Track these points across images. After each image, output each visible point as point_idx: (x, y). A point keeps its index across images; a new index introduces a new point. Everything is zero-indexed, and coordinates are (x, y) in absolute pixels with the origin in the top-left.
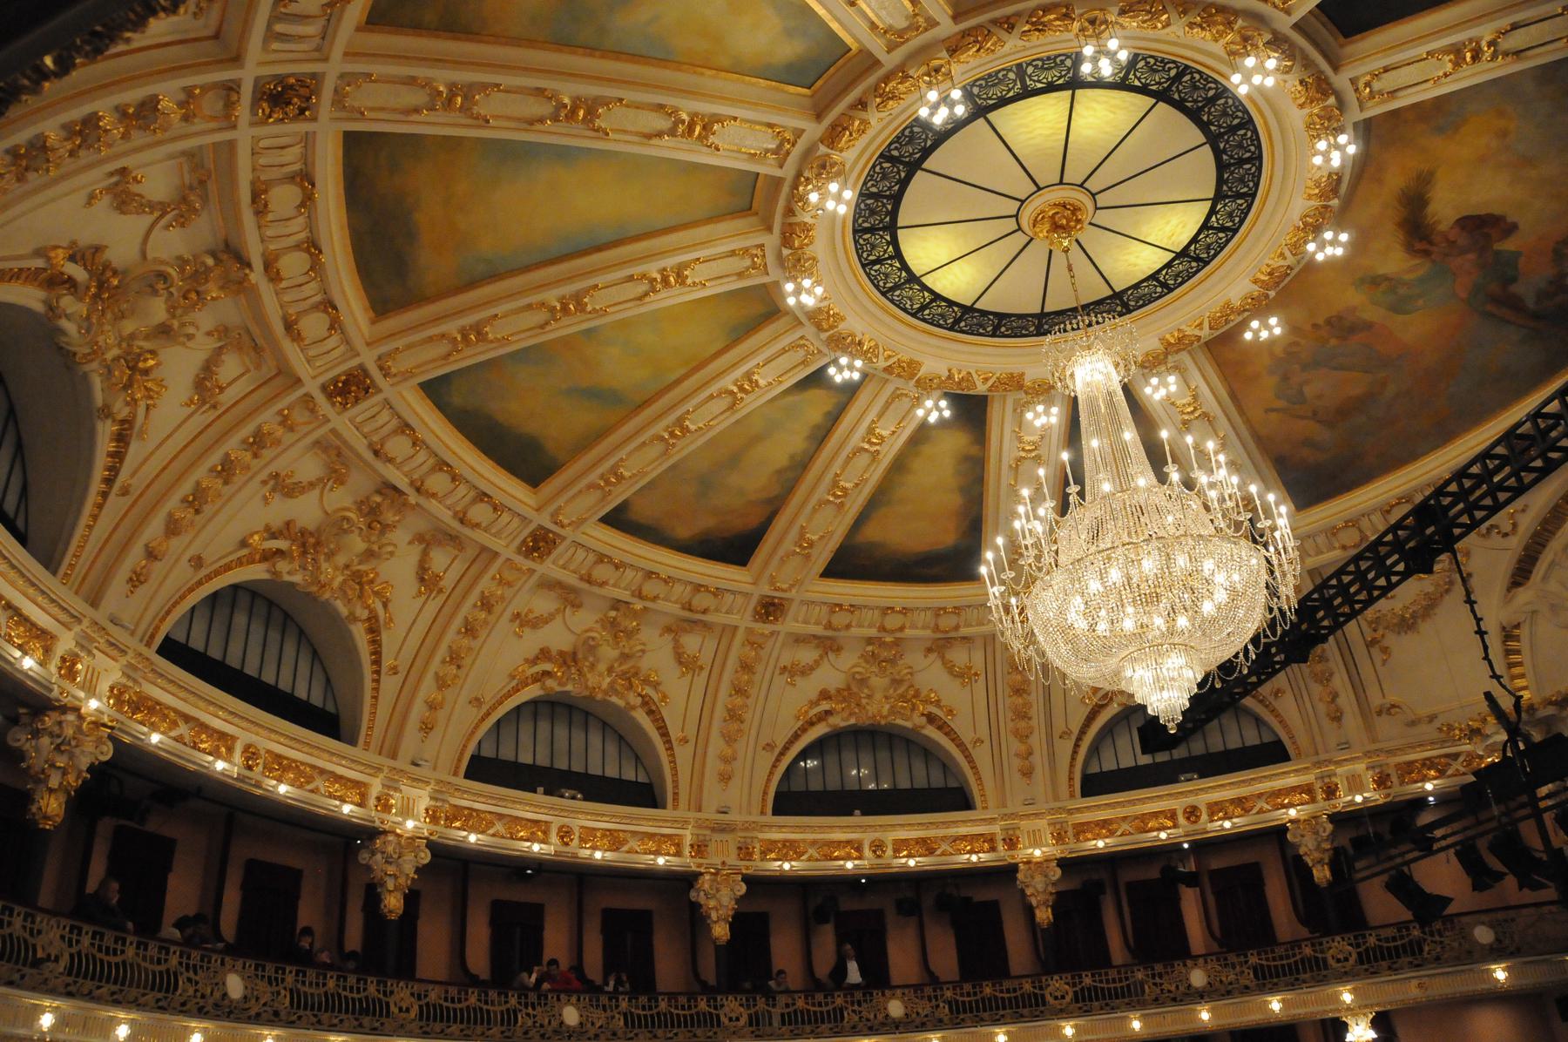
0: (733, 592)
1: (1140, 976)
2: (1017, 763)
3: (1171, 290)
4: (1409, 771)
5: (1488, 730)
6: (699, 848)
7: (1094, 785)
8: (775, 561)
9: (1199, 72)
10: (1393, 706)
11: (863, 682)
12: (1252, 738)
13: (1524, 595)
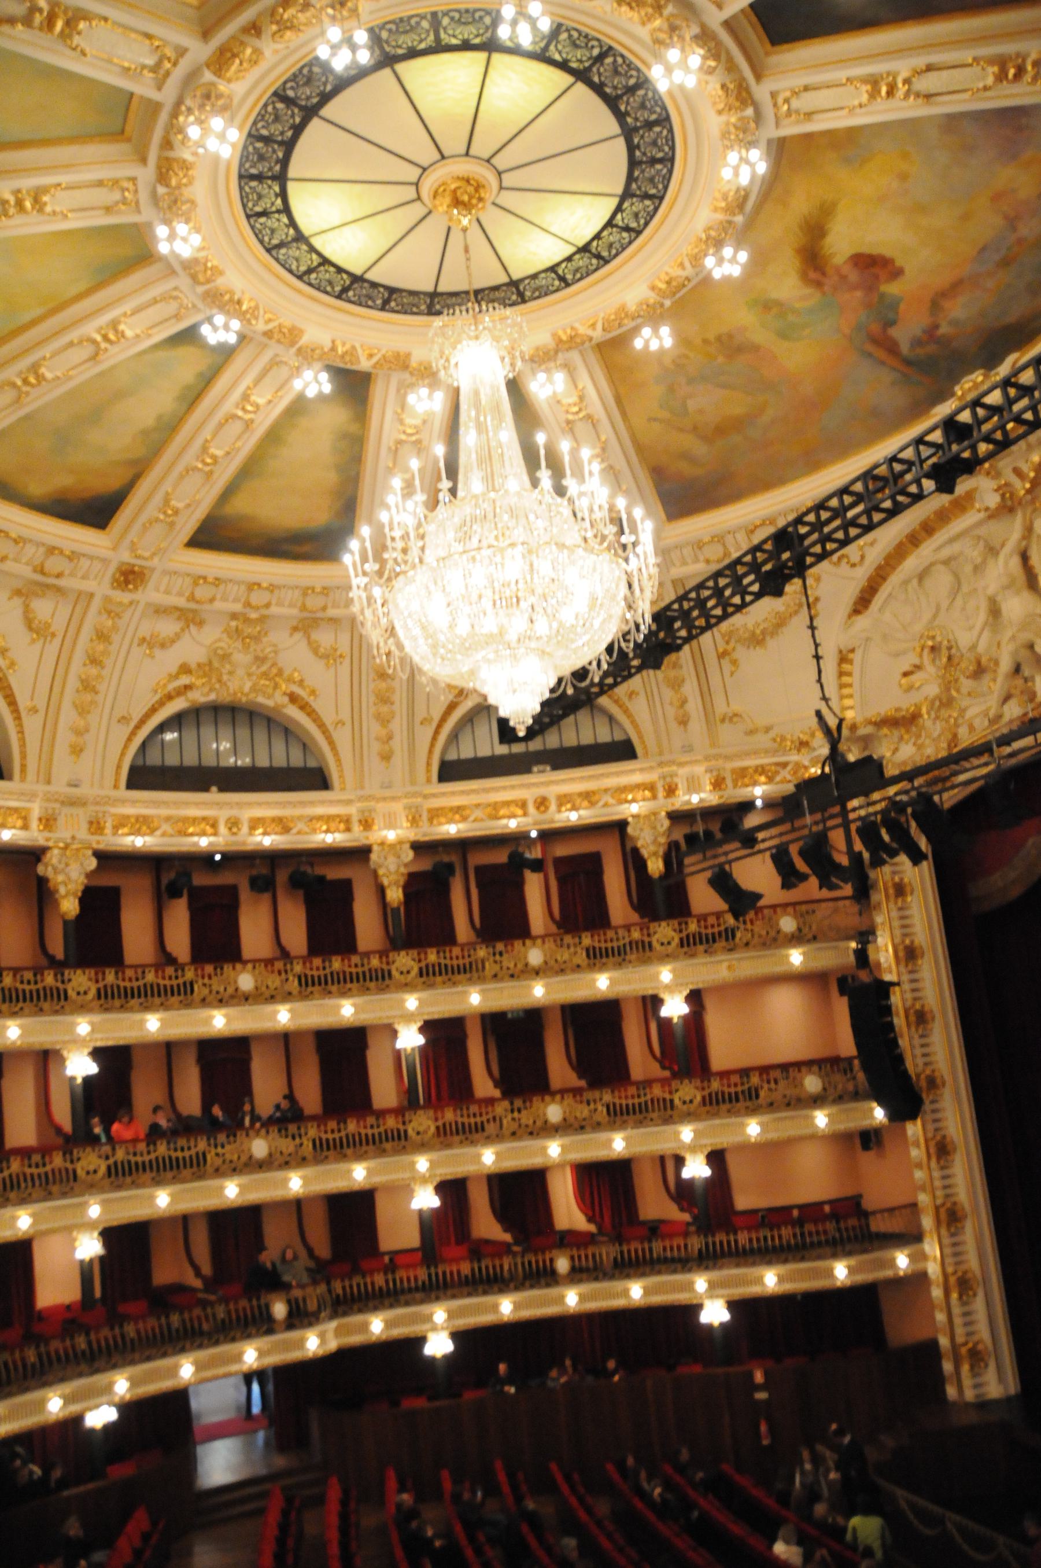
0: (91, 558)
1: (482, 952)
2: (376, 747)
3: (568, 285)
4: (742, 775)
6: (48, 822)
8: (137, 526)
9: (622, 56)
10: (736, 715)
11: (225, 657)
12: (604, 735)
13: (862, 622)
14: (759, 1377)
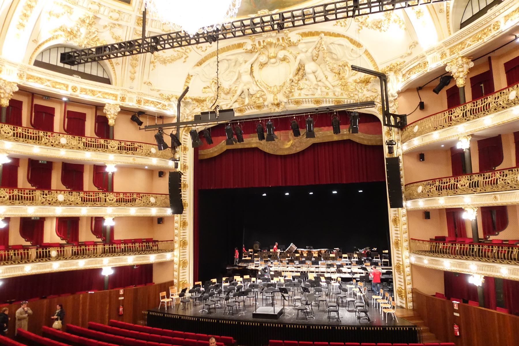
5: (172, 100)
7: (38, 64)
12: (100, 74)
14: (121, 292)
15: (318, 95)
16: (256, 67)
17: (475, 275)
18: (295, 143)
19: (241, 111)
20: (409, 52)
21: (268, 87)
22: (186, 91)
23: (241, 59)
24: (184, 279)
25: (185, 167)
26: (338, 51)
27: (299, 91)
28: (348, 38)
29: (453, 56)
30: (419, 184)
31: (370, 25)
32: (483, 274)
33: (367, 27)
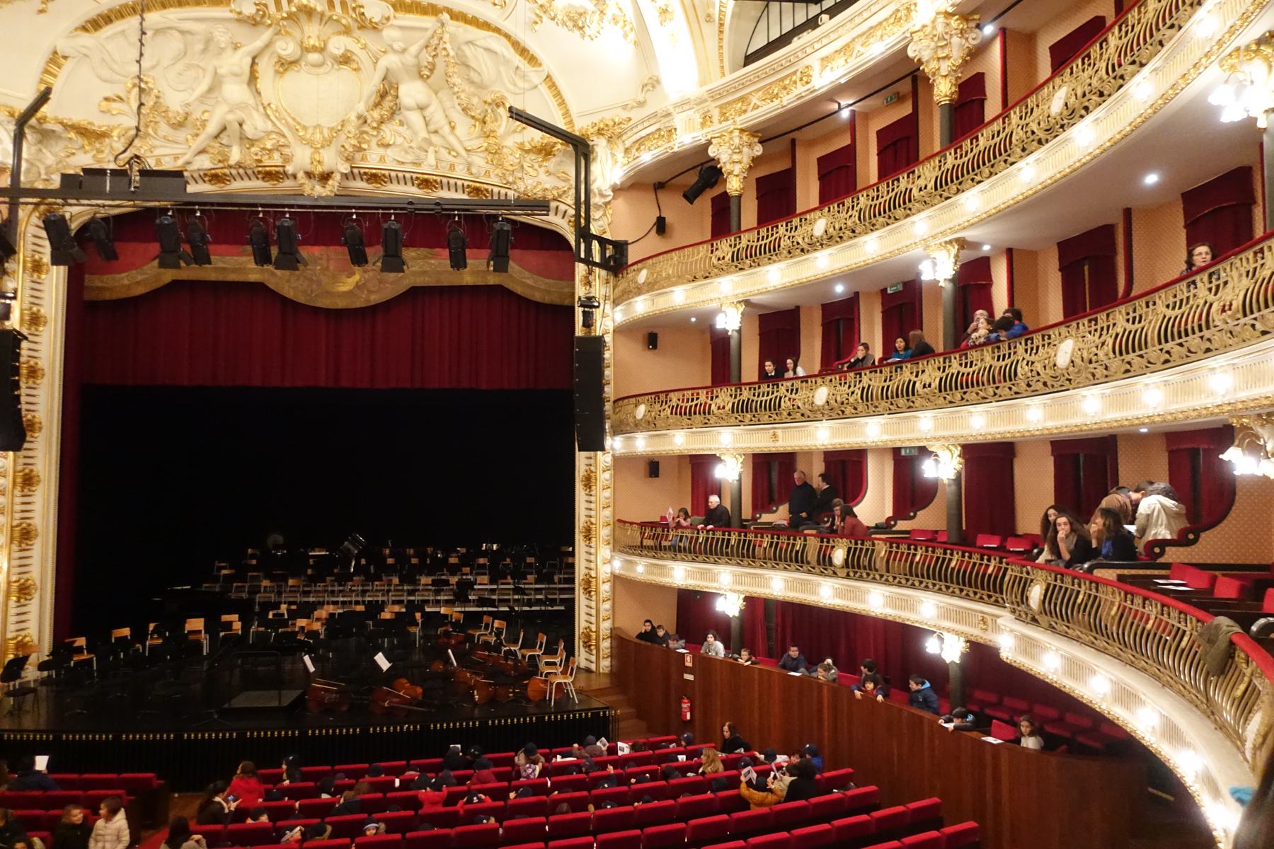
13: (87, 40)
15: (428, 167)
16: (266, 67)
17: (729, 594)
18: (367, 281)
19: (215, 178)
20: (641, 99)
21: (297, 127)
22: (44, 98)
23: (222, 35)
24: (23, 633)
25: (35, 320)
26: (485, 66)
27: (382, 151)
28: (507, 36)
29: (725, 124)
30: (640, 399)
31: (560, 17)
32: (742, 592)
33: (553, 19)
